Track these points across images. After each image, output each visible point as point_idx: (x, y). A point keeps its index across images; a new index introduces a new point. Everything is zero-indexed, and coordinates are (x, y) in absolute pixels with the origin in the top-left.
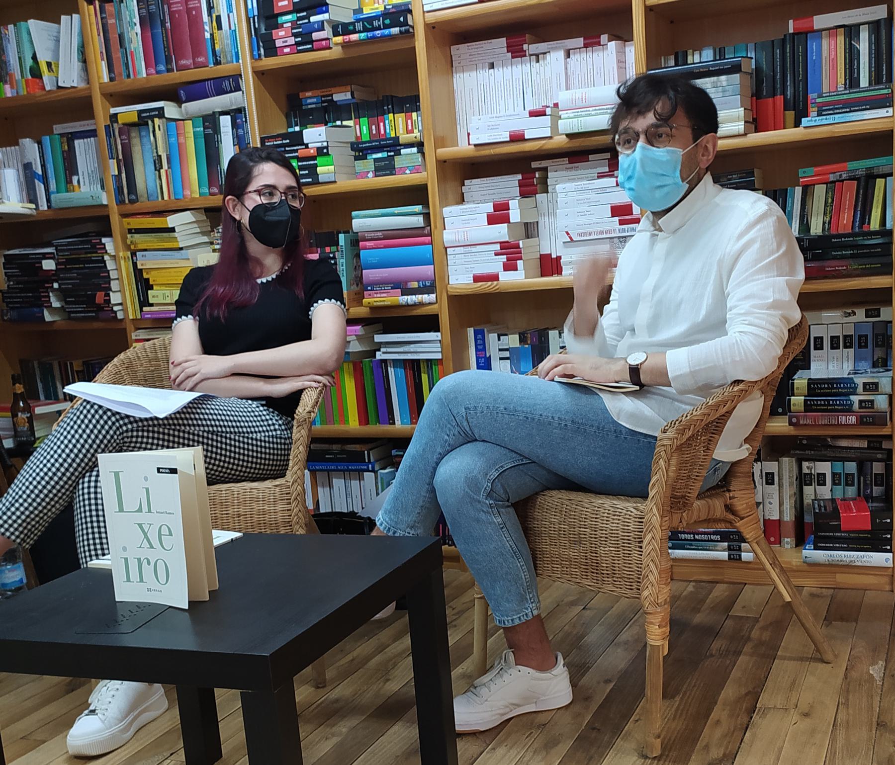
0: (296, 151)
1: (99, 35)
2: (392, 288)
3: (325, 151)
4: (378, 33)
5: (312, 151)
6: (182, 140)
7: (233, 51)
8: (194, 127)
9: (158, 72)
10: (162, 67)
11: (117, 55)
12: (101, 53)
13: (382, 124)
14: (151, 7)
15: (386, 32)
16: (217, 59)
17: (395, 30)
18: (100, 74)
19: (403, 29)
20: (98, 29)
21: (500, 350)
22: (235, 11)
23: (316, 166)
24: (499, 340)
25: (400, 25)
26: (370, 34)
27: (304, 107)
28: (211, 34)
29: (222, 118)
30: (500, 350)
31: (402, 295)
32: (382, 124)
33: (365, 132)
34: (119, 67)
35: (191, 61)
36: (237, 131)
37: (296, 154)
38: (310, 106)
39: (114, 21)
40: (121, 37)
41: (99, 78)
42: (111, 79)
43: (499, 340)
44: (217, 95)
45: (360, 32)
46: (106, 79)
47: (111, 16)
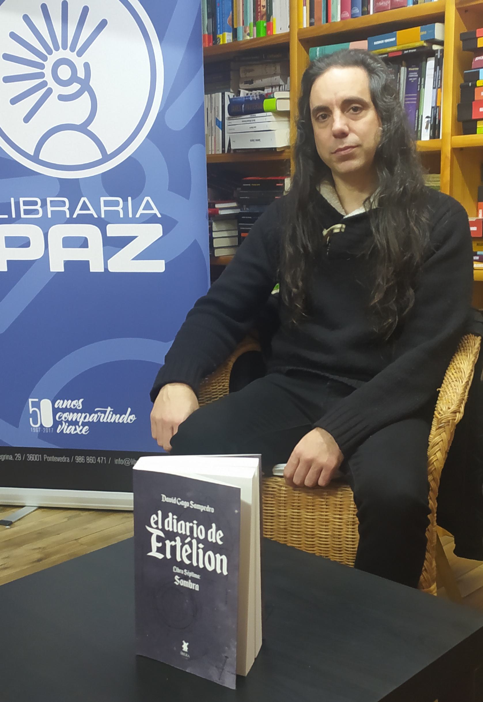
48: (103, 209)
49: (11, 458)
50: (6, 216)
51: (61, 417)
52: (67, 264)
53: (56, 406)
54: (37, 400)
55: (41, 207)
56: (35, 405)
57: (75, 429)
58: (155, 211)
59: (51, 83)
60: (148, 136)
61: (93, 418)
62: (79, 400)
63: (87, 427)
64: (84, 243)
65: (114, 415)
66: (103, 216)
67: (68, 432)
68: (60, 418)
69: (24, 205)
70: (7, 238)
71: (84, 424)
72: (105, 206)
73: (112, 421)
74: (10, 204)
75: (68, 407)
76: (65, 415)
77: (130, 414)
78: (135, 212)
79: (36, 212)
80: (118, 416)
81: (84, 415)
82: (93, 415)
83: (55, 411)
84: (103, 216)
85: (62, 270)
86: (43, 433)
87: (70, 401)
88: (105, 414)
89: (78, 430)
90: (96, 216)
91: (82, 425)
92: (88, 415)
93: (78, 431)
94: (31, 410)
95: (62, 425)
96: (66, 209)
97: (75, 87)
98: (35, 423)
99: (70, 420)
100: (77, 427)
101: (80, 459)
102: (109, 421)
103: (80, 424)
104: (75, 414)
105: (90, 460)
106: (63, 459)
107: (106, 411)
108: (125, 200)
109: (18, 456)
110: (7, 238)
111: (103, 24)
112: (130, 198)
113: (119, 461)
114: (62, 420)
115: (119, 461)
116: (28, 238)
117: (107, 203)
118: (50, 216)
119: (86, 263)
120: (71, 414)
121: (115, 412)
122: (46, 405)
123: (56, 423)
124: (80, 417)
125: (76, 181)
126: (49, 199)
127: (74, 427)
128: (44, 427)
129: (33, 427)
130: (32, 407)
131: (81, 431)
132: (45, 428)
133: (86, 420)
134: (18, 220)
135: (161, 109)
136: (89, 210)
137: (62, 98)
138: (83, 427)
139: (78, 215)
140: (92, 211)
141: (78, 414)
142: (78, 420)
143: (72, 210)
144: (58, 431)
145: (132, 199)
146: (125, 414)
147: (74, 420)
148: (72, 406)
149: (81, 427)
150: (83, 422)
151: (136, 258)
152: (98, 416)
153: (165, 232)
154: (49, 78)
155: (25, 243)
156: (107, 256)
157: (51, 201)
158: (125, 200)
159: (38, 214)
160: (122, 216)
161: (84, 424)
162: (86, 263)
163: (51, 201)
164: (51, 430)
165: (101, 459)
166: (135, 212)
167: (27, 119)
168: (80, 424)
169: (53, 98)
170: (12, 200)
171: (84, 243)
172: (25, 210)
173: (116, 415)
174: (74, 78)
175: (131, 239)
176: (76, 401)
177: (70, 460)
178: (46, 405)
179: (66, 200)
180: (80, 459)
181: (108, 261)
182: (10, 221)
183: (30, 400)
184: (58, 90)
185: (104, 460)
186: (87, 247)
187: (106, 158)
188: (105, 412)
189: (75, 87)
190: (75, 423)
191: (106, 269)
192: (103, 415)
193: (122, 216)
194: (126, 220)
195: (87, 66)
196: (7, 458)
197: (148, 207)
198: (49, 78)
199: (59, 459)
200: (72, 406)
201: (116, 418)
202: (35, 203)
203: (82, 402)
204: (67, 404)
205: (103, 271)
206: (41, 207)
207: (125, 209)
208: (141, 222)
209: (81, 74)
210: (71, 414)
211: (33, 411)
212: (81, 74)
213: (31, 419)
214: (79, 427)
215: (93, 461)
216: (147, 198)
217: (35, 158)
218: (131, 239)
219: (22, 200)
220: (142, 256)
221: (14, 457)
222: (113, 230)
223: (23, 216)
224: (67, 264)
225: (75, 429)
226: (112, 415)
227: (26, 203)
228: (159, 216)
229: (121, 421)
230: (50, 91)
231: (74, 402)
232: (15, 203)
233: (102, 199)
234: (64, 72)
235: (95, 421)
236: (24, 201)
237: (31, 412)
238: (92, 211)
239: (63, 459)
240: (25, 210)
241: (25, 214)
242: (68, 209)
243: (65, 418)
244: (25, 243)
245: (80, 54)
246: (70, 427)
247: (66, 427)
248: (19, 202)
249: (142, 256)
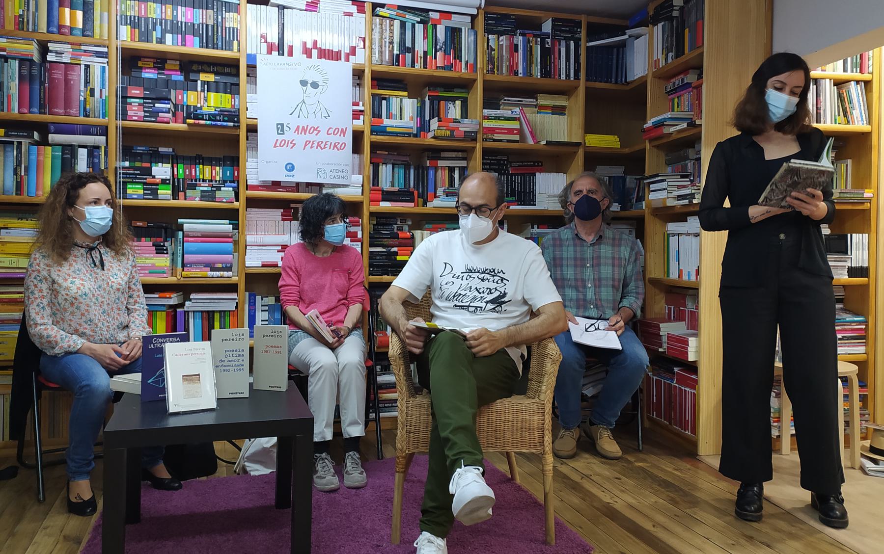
0: (146, 179)
2: (204, 267)
3: (168, 182)
4: (219, 123)
5: (158, 181)
6: (41, 158)
7: (101, 112)
8: (52, 151)
9: (30, 112)
10: (36, 110)
13: (193, 170)
14: (33, 71)
15: (225, 124)
16: (86, 114)
17: (231, 124)
19: (236, 124)
21: (262, 306)
22: (107, 88)
23: (158, 189)
24: (262, 300)
25: (234, 122)
26: (213, 123)
27: (133, 151)
28: (84, 98)
29: (80, 150)
30: (262, 306)
31: (211, 271)
32: (193, 170)
33: (181, 173)
36: (93, 159)
37: (145, 181)
38: (138, 151)
43: (262, 300)
44: (83, 135)
45: (206, 120)
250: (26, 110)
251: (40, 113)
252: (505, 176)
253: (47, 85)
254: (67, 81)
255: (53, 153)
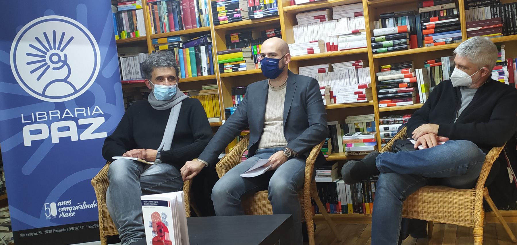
1: (151, 17)
10: (177, 29)
11: (158, 24)
12: (151, 23)
14: (173, 6)
18: (151, 31)
20: (150, 15)
34: (159, 29)
35: (191, 26)
39: (157, 11)
40: (160, 18)
41: (150, 33)
42: (156, 33)
46: (153, 33)
47: (156, 10)
48: (76, 113)
49: (36, 234)
50: (30, 121)
51: (61, 210)
52: (60, 139)
53: (58, 205)
54: (48, 204)
55: (47, 115)
56: (48, 206)
57: (68, 215)
58: (101, 112)
59: (49, 63)
60: (95, 81)
61: (77, 208)
62: (69, 201)
63: (74, 213)
64: (68, 129)
65: (87, 205)
66: (76, 116)
67: (65, 216)
68: (60, 210)
69: (38, 115)
70: (30, 131)
71: (72, 212)
72: (77, 112)
73: (86, 208)
74: (32, 115)
75: (64, 204)
76: (63, 208)
77: (95, 204)
78: (91, 113)
79: (44, 118)
80: (89, 205)
81: (72, 207)
82: (77, 206)
83: (58, 207)
84: (76, 116)
85: (58, 142)
86: (52, 219)
87: (65, 202)
88: (83, 205)
89: (70, 215)
90: (73, 117)
91: (71, 212)
92: (74, 207)
93: (70, 215)
94: (46, 209)
95: (61, 214)
96: (58, 115)
97: (61, 64)
98: (48, 215)
99: (65, 210)
100: (69, 213)
101: (71, 229)
102: (84, 208)
103: (71, 212)
104: (68, 207)
105: (77, 228)
106: (64, 230)
107: (83, 204)
108: (86, 109)
109: (40, 232)
110: (30, 131)
111: (72, 38)
112: (88, 108)
113: (91, 227)
114: (62, 211)
115: (91, 227)
116: (41, 130)
117: (78, 111)
118: (51, 119)
119: (70, 137)
120: (66, 208)
121: (87, 204)
122: (53, 205)
123: (59, 213)
124: (70, 209)
125: (63, 103)
126: (50, 112)
127: (68, 214)
128: (53, 216)
129: (47, 217)
130: (46, 207)
131: (71, 215)
132: (53, 216)
133: (74, 209)
134: (36, 122)
135: (100, 70)
136: (70, 114)
137: (54, 69)
138: (72, 213)
139: (65, 117)
140: (71, 115)
141: (69, 207)
142: (69, 210)
143: (61, 115)
144: (60, 217)
145: (90, 108)
146: (92, 204)
147: (67, 210)
148: (66, 204)
149: (71, 213)
150: (72, 211)
151: (92, 133)
152: (79, 206)
153: (106, 120)
154: (48, 61)
155: (40, 132)
156: (79, 134)
157: (51, 113)
158: (86, 109)
159: (45, 118)
160: (85, 115)
161: (72, 212)
162: (70, 137)
163: (51, 113)
164: (56, 217)
165: (82, 227)
166: (91, 113)
167: (38, 79)
168: (71, 212)
169: (51, 69)
170: (33, 114)
171: (68, 129)
172: (39, 118)
173: (88, 205)
174: (60, 60)
175: (91, 124)
176: (68, 201)
177: (67, 230)
178: (53, 205)
179: (58, 111)
180: (71, 229)
181: (80, 136)
182: (32, 123)
183: (45, 204)
184: (52, 66)
185: (83, 227)
186: (70, 130)
187: (76, 91)
188: (82, 204)
189: (61, 64)
190: (68, 212)
191: (79, 139)
192: (82, 206)
193: (85, 115)
194: (87, 117)
195: (65, 55)
196: (34, 234)
197: (97, 110)
198: (48, 61)
199: (61, 230)
200: (66, 204)
201: (88, 206)
202: (44, 114)
203: (71, 201)
204: (64, 203)
205: (78, 140)
206: (47, 115)
207: (87, 112)
208: (95, 116)
209: (63, 58)
210: (66, 208)
211: (47, 209)
212: (63, 58)
213: (46, 213)
214: (70, 213)
215: (78, 229)
216: (96, 107)
217: (43, 95)
218: (91, 124)
219: (37, 113)
220: (96, 131)
221: (38, 233)
222: (81, 122)
223: (38, 120)
224: (60, 139)
225: (68, 215)
226: (86, 205)
227: (39, 115)
228: (103, 113)
229: (90, 207)
230: (49, 67)
231: (67, 202)
232: (34, 115)
233: (75, 109)
234: (55, 59)
235: (78, 209)
236: (38, 114)
237: (46, 210)
238: (71, 115)
239: (64, 230)
240: (39, 118)
241: (39, 119)
242: (60, 115)
243: (63, 210)
244: (40, 132)
245: (62, 51)
246: (66, 214)
247: (64, 214)
248: (36, 114)
249: (96, 131)
250: (173, 30)
251: (180, 30)
252: (498, 8)
253: (182, 13)
254: (191, 8)
255: (190, 52)
